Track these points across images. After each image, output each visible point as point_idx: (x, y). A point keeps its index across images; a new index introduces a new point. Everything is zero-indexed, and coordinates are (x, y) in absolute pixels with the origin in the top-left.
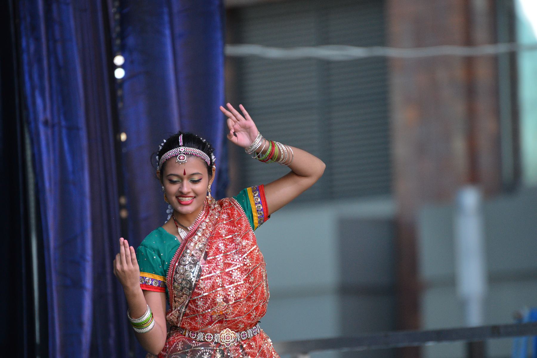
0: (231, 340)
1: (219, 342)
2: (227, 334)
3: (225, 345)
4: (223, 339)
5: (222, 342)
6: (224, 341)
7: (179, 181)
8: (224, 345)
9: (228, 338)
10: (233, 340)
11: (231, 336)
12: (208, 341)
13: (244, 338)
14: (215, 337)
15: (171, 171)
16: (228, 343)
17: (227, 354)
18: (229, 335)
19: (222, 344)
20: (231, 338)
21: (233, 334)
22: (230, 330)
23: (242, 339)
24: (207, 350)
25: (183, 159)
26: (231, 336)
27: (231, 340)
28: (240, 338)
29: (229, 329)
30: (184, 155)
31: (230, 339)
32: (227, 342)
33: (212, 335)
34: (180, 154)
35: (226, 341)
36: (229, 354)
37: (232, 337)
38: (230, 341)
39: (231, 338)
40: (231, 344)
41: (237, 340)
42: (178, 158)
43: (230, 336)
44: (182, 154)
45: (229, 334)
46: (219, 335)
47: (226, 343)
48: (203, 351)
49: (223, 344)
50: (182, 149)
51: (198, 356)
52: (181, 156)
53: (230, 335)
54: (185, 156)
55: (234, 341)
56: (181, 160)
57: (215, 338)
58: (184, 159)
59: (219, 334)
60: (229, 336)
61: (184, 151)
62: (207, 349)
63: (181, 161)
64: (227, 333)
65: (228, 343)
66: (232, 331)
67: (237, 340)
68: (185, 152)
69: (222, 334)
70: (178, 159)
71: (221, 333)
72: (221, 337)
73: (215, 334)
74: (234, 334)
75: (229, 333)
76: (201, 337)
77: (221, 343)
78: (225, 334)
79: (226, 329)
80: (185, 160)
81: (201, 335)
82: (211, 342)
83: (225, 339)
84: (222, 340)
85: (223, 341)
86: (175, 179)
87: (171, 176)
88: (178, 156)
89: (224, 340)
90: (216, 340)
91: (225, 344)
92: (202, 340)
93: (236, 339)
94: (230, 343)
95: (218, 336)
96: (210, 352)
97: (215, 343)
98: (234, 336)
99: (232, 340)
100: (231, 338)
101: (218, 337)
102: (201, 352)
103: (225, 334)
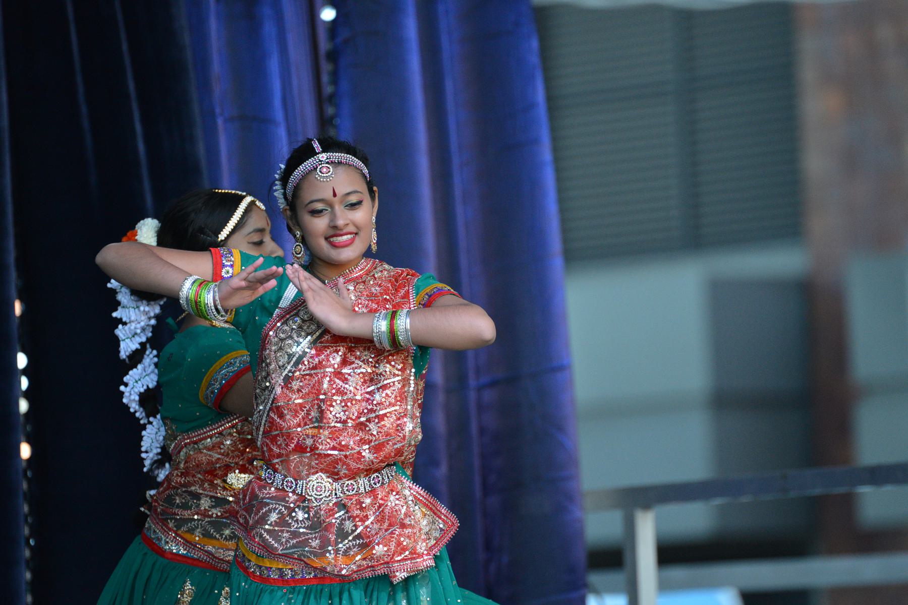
1: (304, 494)
3: (313, 500)
5: (308, 495)
6: (313, 494)
7: (327, 210)
8: (312, 499)
9: (319, 489)
10: (329, 494)
12: (287, 490)
13: (351, 491)
14: (299, 485)
16: (318, 497)
18: (322, 485)
19: (309, 498)
20: (325, 491)
22: (324, 476)
24: (277, 506)
25: (327, 172)
28: (341, 493)
29: (322, 475)
30: (329, 166)
32: (317, 495)
33: (294, 482)
34: (321, 164)
35: (316, 495)
37: (327, 488)
38: (321, 495)
39: (324, 489)
40: (323, 500)
41: (336, 494)
42: (318, 171)
43: (323, 487)
44: (324, 164)
45: (322, 483)
47: (314, 498)
49: (310, 498)
50: (323, 157)
52: (324, 167)
53: (324, 485)
54: (331, 167)
55: (329, 496)
56: (323, 174)
57: (298, 487)
58: (329, 171)
59: (304, 481)
61: (327, 159)
62: (279, 505)
63: (325, 175)
64: (318, 481)
65: (318, 497)
66: (328, 477)
67: (336, 494)
68: (328, 160)
69: (309, 482)
70: (319, 173)
71: (308, 480)
72: (308, 486)
73: (298, 481)
74: (330, 483)
75: (322, 481)
77: (307, 496)
78: (315, 483)
80: (331, 173)
83: (314, 490)
84: (309, 492)
85: (310, 494)
86: (319, 206)
88: (319, 167)
90: (299, 491)
91: (313, 498)
93: (334, 492)
94: (322, 498)
95: (303, 484)
96: (281, 509)
97: (298, 494)
98: (330, 487)
100: (325, 491)
101: (302, 487)
103: (315, 481)
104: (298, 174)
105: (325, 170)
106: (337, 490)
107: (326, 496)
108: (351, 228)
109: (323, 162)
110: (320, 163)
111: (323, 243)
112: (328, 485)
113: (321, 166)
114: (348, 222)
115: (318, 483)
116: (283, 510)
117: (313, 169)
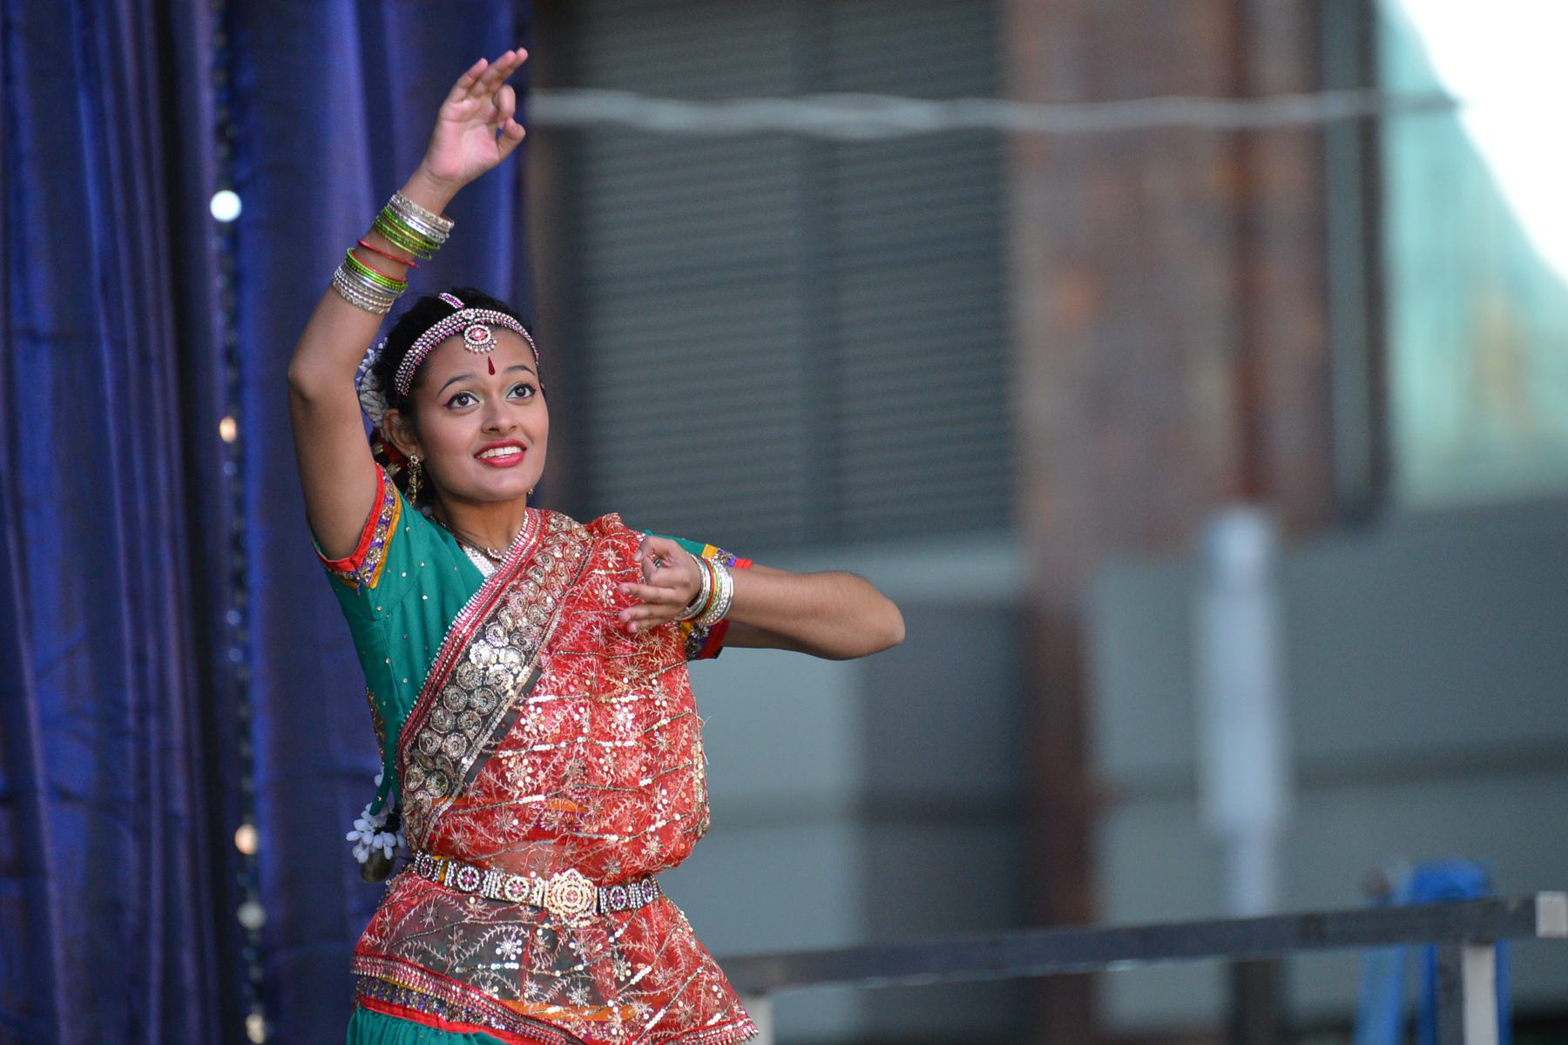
0: (581, 903)
1: (546, 905)
3: (562, 915)
4: (559, 898)
5: (553, 906)
6: (561, 906)
9: (572, 897)
10: (587, 906)
11: (581, 892)
12: (512, 899)
13: (619, 904)
15: (439, 374)
16: (570, 911)
17: (568, 942)
22: (580, 877)
23: (612, 908)
24: (510, 928)
26: (581, 892)
27: (581, 903)
28: (607, 905)
29: (576, 872)
32: (569, 907)
36: (572, 945)
37: (585, 896)
40: (577, 918)
42: (467, 338)
43: (579, 894)
46: (547, 885)
48: (501, 931)
49: (557, 912)
51: (485, 941)
55: (588, 910)
63: (481, 343)
67: (598, 909)
69: (555, 883)
71: (553, 880)
72: (554, 891)
75: (577, 884)
76: (494, 885)
77: (550, 909)
78: (565, 885)
79: (569, 872)
80: (489, 338)
81: (494, 882)
82: (522, 904)
83: (564, 898)
84: (554, 901)
85: (556, 905)
87: (448, 387)
89: (560, 902)
90: (536, 900)
92: (494, 895)
93: (595, 904)
96: (519, 932)
97: (534, 907)
98: (590, 896)
102: (492, 932)
103: (566, 884)
104: (424, 343)
105: (478, 334)
106: (601, 901)
107: (582, 910)
108: (519, 436)
109: (469, 323)
110: (465, 323)
111: (469, 464)
112: (586, 891)
113: (469, 329)
114: (516, 423)
115: (571, 885)
116: (523, 932)
117: (443, 338)
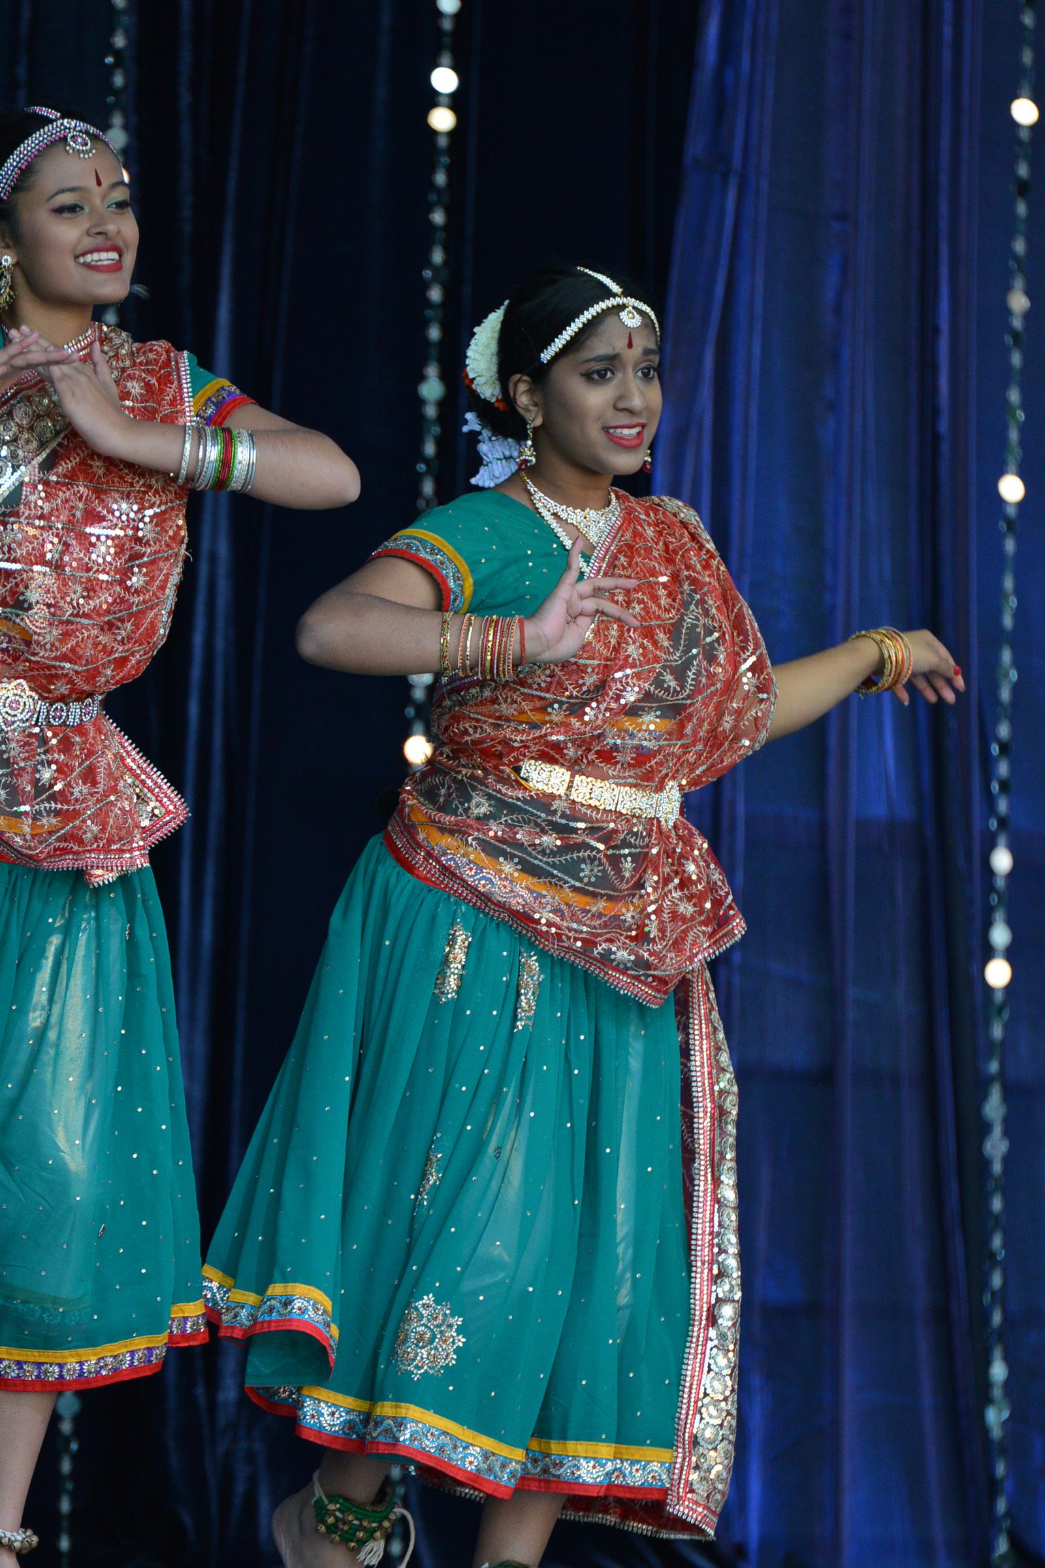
2: (15, 695)
9: (14, 705)
11: (25, 703)
16: (9, 718)
20: (23, 710)
21: (31, 700)
23: (50, 722)
26: (25, 703)
27: (21, 713)
31: (20, 711)
35: (7, 713)
38: (16, 716)
40: (15, 725)
43: (22, 704)
55: (27, 720)
60: (18, 702)
64: (16, 692)
65: (9, 718)
66: (31, 689)
75: (23, 694)
78: (10, 694)
99: (22, 716)
100: (23, 710)
103: (12, 692)
